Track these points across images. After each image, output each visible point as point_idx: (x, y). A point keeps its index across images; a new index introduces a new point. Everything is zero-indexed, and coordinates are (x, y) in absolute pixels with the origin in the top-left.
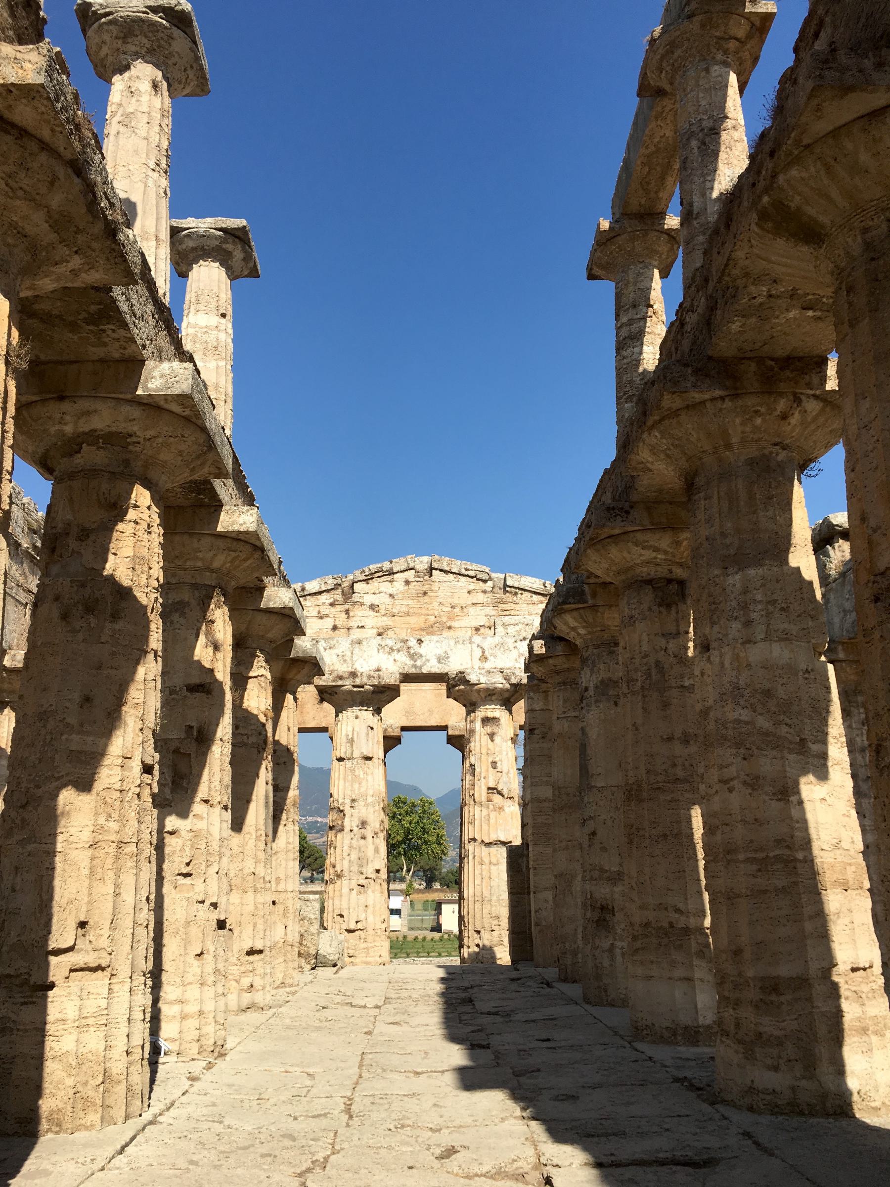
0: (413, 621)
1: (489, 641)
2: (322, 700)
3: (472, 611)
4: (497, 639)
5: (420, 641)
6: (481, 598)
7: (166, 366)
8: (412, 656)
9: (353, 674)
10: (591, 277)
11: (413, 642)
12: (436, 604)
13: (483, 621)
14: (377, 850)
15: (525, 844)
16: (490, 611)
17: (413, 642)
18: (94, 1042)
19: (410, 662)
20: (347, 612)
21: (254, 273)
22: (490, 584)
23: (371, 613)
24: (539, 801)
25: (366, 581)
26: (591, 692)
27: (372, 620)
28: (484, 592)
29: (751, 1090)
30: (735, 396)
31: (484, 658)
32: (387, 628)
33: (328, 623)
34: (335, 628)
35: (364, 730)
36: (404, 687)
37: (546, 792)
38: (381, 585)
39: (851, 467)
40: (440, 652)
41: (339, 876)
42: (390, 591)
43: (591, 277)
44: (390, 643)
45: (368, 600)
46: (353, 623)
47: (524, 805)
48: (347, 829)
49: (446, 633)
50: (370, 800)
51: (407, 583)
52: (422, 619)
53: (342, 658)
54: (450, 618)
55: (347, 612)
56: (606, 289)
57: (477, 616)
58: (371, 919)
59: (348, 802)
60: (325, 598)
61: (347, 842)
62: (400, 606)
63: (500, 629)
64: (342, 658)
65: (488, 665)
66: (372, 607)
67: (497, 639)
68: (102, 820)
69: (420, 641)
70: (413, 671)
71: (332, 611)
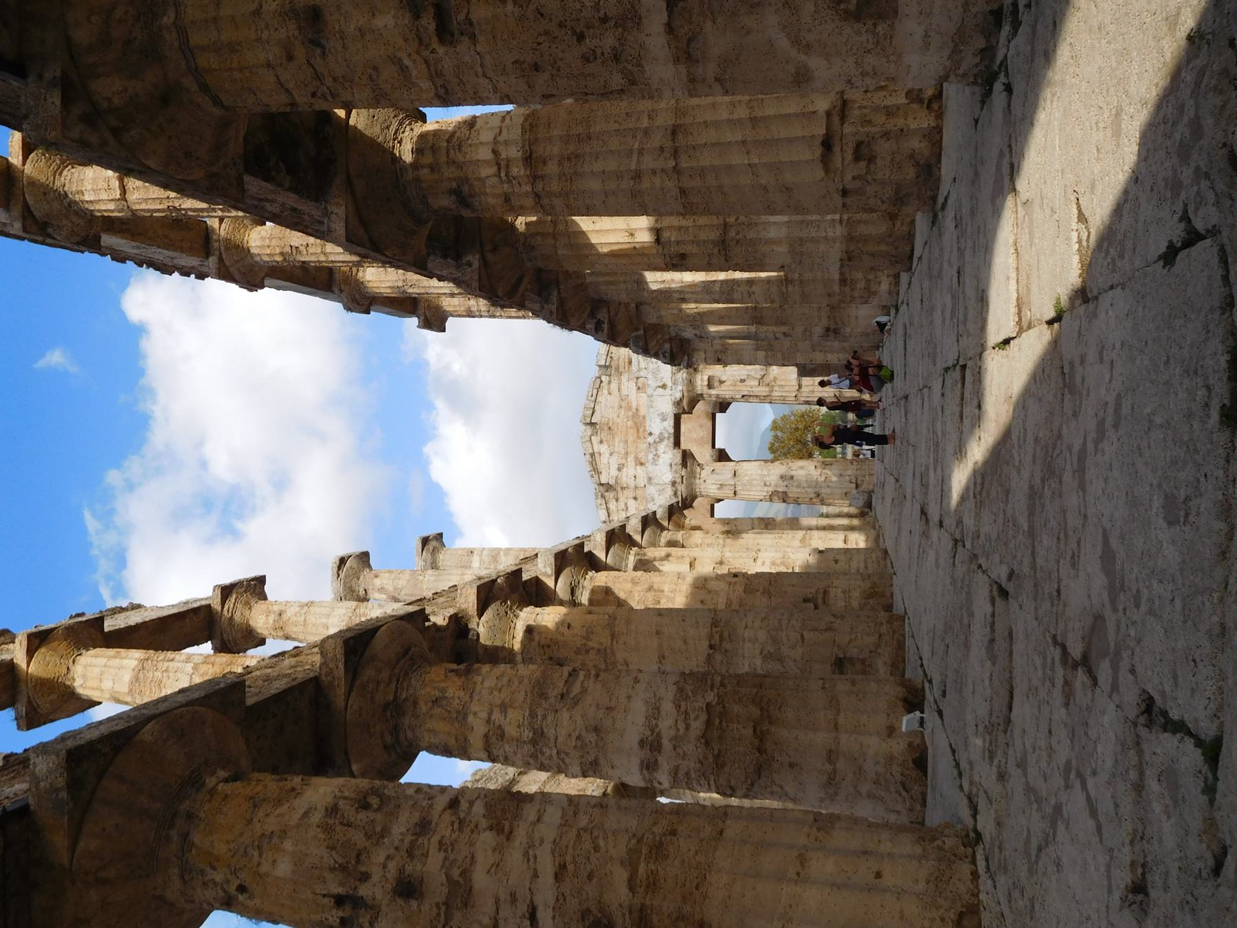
0: (631, 439)
1: (652, 382)
2: (691, 506)
3: (624, 392)
4: (650, 376)
5: (651, 434)
6: (614, 386)
7: (540, 566)
8: (661, 440)
9: (674, 483)
10: (444, 330)
11: (651, 439)
12: (619, 420)
13: (632, 385)
14: (802, 468)
15: (797, 365)
16: (624, 378)
17: (651, 439)
18: (856, 594)
19: (666, 442)
20: (623, 488)
21: (441, 535)
22: (603, 378)
23: (624, 470)
24: (766, 357)
25: (599, 473)
26: (697, 332)
27: (630, 470)
28: (610, 382)
29: (890, 293)
30: (558, 283)
31: (664, 386)
32: (636, 458)
33: (631, 503)
34: (635, 498)
35: (715, 476)
36: (683, 446)
37: (761, 354)
38: (603, 461)
39: (589, 212)
40: (658, 420)
41: (818, 495)
42: (607, 455)
43: (444, 330)
44: (651, 456)
45: (614, 472)
46: (632, 483)
47: (768, 364)
48: (785, 489)
49: (642, 413)
50: (765, 472)
51: (601, 442)
52: (631, 431)
53: (661, 492)
54: (629, 408)
55: (623, 488)
56: (450, 322)
57: (629, 387)
58: (849, 472)
59: (766, 489)
60: (612, 505)
61: (795, 490)
62: (619, 447)
63: (642, 374)
64: (661, 492)
65: (669, 384)
66: (619, 470)
67: (650, 376)
68: (758, 594)
69: (651, 434)
70: (672, 439)
71: (622, 499)
